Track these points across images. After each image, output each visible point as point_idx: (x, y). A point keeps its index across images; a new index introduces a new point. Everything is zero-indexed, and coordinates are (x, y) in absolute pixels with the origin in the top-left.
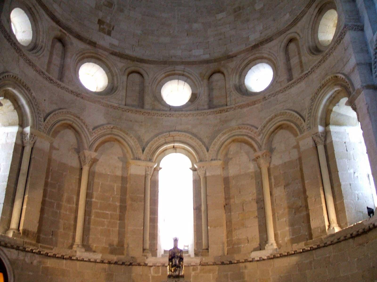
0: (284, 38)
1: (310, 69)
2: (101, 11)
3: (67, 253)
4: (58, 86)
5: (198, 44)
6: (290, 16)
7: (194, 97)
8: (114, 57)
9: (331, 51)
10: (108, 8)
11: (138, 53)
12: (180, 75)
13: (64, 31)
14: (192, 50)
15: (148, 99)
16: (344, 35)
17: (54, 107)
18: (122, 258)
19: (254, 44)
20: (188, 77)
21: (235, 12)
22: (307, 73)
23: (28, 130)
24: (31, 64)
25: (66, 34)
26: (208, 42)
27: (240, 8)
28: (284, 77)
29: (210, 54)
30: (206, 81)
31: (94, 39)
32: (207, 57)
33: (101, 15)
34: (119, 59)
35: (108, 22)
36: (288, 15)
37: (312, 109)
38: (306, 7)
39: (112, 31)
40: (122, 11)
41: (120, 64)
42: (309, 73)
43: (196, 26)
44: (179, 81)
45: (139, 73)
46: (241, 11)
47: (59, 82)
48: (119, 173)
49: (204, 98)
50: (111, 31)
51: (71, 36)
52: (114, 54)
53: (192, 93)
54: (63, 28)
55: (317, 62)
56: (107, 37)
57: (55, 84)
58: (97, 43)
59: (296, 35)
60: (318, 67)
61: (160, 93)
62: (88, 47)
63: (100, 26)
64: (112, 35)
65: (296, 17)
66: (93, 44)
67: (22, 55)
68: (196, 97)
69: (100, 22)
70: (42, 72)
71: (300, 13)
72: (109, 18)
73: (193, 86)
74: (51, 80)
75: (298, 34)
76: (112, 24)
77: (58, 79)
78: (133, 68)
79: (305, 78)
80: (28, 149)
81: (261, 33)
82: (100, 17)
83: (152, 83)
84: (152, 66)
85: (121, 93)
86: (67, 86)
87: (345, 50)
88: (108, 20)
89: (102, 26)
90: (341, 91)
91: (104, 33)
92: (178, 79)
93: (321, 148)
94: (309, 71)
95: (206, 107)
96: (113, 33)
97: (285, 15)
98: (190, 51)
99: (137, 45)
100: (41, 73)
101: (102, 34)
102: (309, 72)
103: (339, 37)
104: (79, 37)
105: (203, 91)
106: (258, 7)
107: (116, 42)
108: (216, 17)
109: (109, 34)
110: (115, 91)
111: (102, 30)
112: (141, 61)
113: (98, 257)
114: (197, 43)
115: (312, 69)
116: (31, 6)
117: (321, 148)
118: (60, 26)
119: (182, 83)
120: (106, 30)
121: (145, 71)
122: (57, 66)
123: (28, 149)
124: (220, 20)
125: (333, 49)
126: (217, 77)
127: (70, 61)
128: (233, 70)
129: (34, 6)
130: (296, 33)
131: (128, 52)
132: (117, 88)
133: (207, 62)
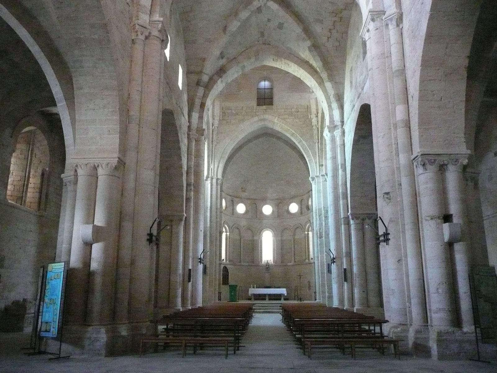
0: (300, 198)
3: (240, 264)
17: (233, 224)
18: (253, 264)
23: (228, 234)
37: (305, 226)
41: (249, 202)
48: (251, 238)
52: (247, 199)
66: (241, 198)
69: (242, 188)
78: (253, 202)
80: (228, 238)
93: (306, 237)
95: (277, 216)
104: (237, 197)
113: (247, 264)
117: (306, 237)
123: (228, 238)
126: (280, 205)
131: (252, 197)
133: (277, 199)
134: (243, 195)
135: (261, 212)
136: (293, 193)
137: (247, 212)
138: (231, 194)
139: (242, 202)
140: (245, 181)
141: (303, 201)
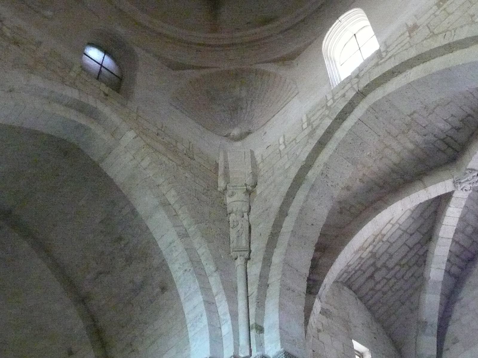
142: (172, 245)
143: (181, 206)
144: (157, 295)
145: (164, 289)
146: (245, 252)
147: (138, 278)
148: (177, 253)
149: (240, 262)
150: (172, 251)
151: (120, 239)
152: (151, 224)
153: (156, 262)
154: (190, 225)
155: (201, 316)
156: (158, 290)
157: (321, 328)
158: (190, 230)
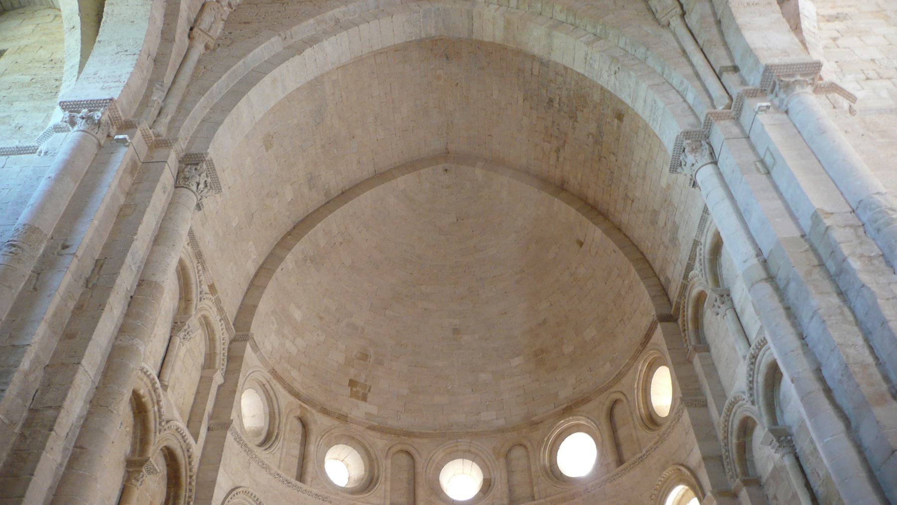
0: (605, 400)
1: (644, 451)
2: (353, 367)
4: (299, 489)
5: (488, 403)
6: (611, 366)
7: (487, 486)
8: (372, 433)
9: (669, 430)
10: (362, 361)
11: (405, 422)
12: (465, 451)
13: (307, 406)
14: (480, 413)
15: (421, 493)
16: (683, 412)
19: (565, 406)
20: (477, 455)
21: (537, 355)
22: (641, 457)
24: (264, 466)
25: (306, 409)
26: (502, 399)
27: (542, 351)
28: (611, 458)
29: (505, 418)
30: (502, 461)
31: (345, 410)
32: (501, 422)
33: (352, 373)
34: (379, 435)
35: (362, 381)
36: (608, 364)
38: (630, 359)
39: (369, 394)
40: (380, 363)
41: (380, 442)
42: (643, 457)
43: (483, 376)
44: (464, 460)
45: (408, 453)
46: (544, 355)
47: (299, 484)
49: (500, 488)
50: (367, 394)
51: (314, 411)
52: (372, 428)
53: (484, 480)
54: (303, 402)
55: (653, 442)
56: (361, 404)
57: (294, 487)
58: (349, 416)
59: (620, 396)
60: (655, 449)
61: (438, 480)
62: (336, 423)
63: (351, 390)
64: (368, 400)
65: (618, 371)
66: (343, 418)
67: (254, 456)
68: (490, 485)
69: (352, 383)
70: (278, 474)
71: (624, 367)
72: (363, 377)
73: (484, 467)
74: (289, 483)
75: (625, 395)
76: (368, 383)
77: (297, 479)
78: (399, 447)
79: (639, 463)
81: (574, 389)
82: (352, 377)
83: (427, 468)
84: (426, 441)
85: (383, 488)
86: (309, 489)
87: (687, 433)
88: (362, 379)
89: (354, 389)
90: (687, 490)
91: (357, 398)
92: (463, 458)
94: (643, 453)
96: (370, 396)
97: (605, 364)
98: (477, 415)
99: (403, 411)
100: (276, 476)
101: (356, 401)
102: (644, 455)
103: (676, 414)
104: (325, 411)
105: (500, 477)
106: (568, 349)
107: (373, 409)
108: (510, 363)
109: (364, 398)
110: (375, 485)
111: (353, 395)
112: (410, 434)
114: (486, 402)
115: (647, 452)
116: (265, 382)
118: (300, 400)
119: (468, 462)
120: (360, 394)
121: (416, 449)
122: (296, 457)
124: (516, 367)
125: (671, 428)
127: (312, 448)
128: (539, 443)
129: (268, 382)
130: (622, 393)
131: (392, 423)
132: (378, 479)
133: (501, 431)
134: (359, 410)
135: (436, 490)
136: (566, 393)
137: (369, 484)
138: (297, 386)
139: (351, 440)
140: (364, 357)
141: (617, 411)
142: (588, 58)
143: (575, 15)
144: (619, 127)
145: (620, 117)
146: (676, 9)
147: (593, 127)
148: (597, 63)
149: (676, 23)
150: (591, 65)
151: (551, 101)
152: (556, 57)
153: (597, 97)
154: (594, 27)
155: (655, 103)
156: (616, 121)
157: (836, 34)
158: (598, 31)
